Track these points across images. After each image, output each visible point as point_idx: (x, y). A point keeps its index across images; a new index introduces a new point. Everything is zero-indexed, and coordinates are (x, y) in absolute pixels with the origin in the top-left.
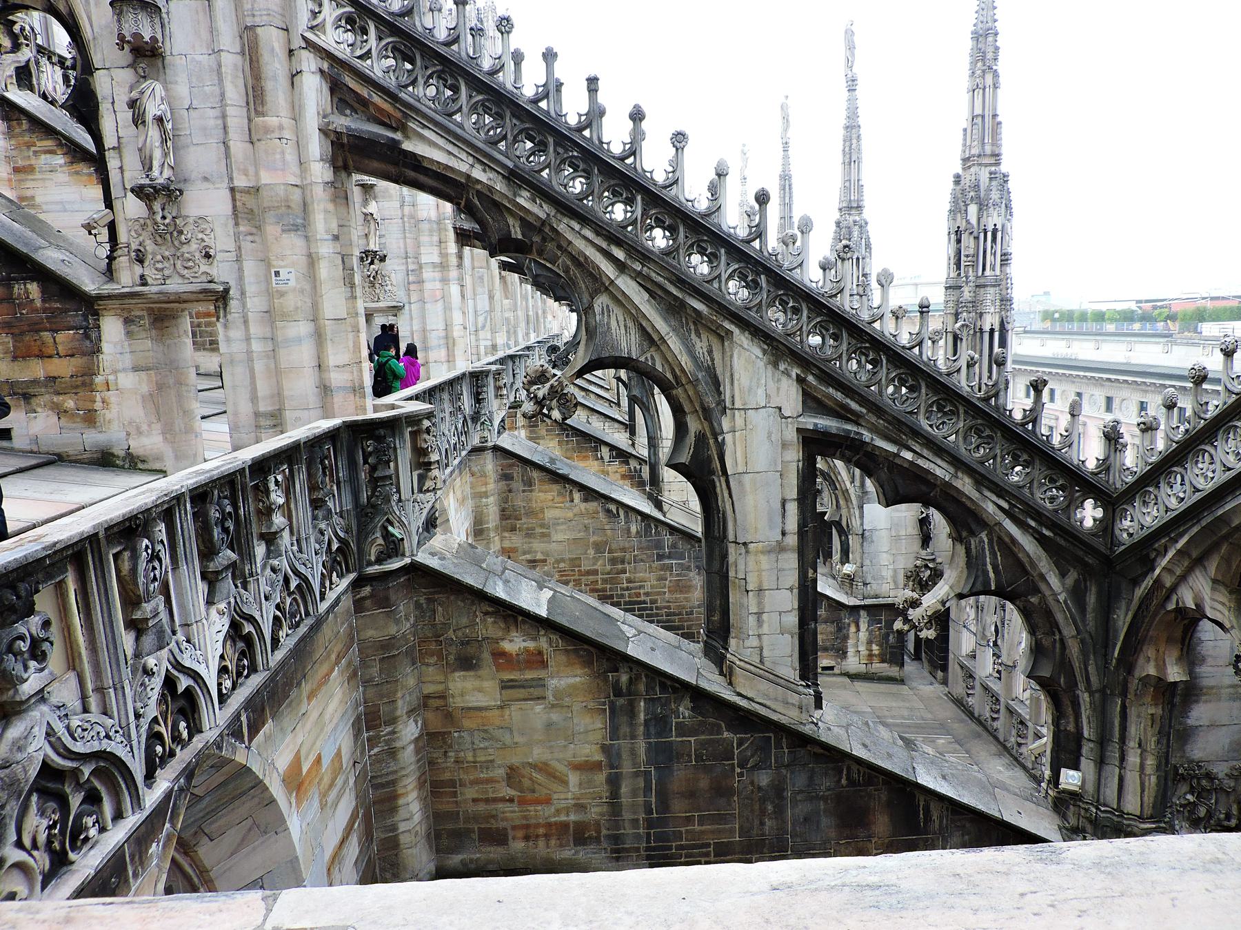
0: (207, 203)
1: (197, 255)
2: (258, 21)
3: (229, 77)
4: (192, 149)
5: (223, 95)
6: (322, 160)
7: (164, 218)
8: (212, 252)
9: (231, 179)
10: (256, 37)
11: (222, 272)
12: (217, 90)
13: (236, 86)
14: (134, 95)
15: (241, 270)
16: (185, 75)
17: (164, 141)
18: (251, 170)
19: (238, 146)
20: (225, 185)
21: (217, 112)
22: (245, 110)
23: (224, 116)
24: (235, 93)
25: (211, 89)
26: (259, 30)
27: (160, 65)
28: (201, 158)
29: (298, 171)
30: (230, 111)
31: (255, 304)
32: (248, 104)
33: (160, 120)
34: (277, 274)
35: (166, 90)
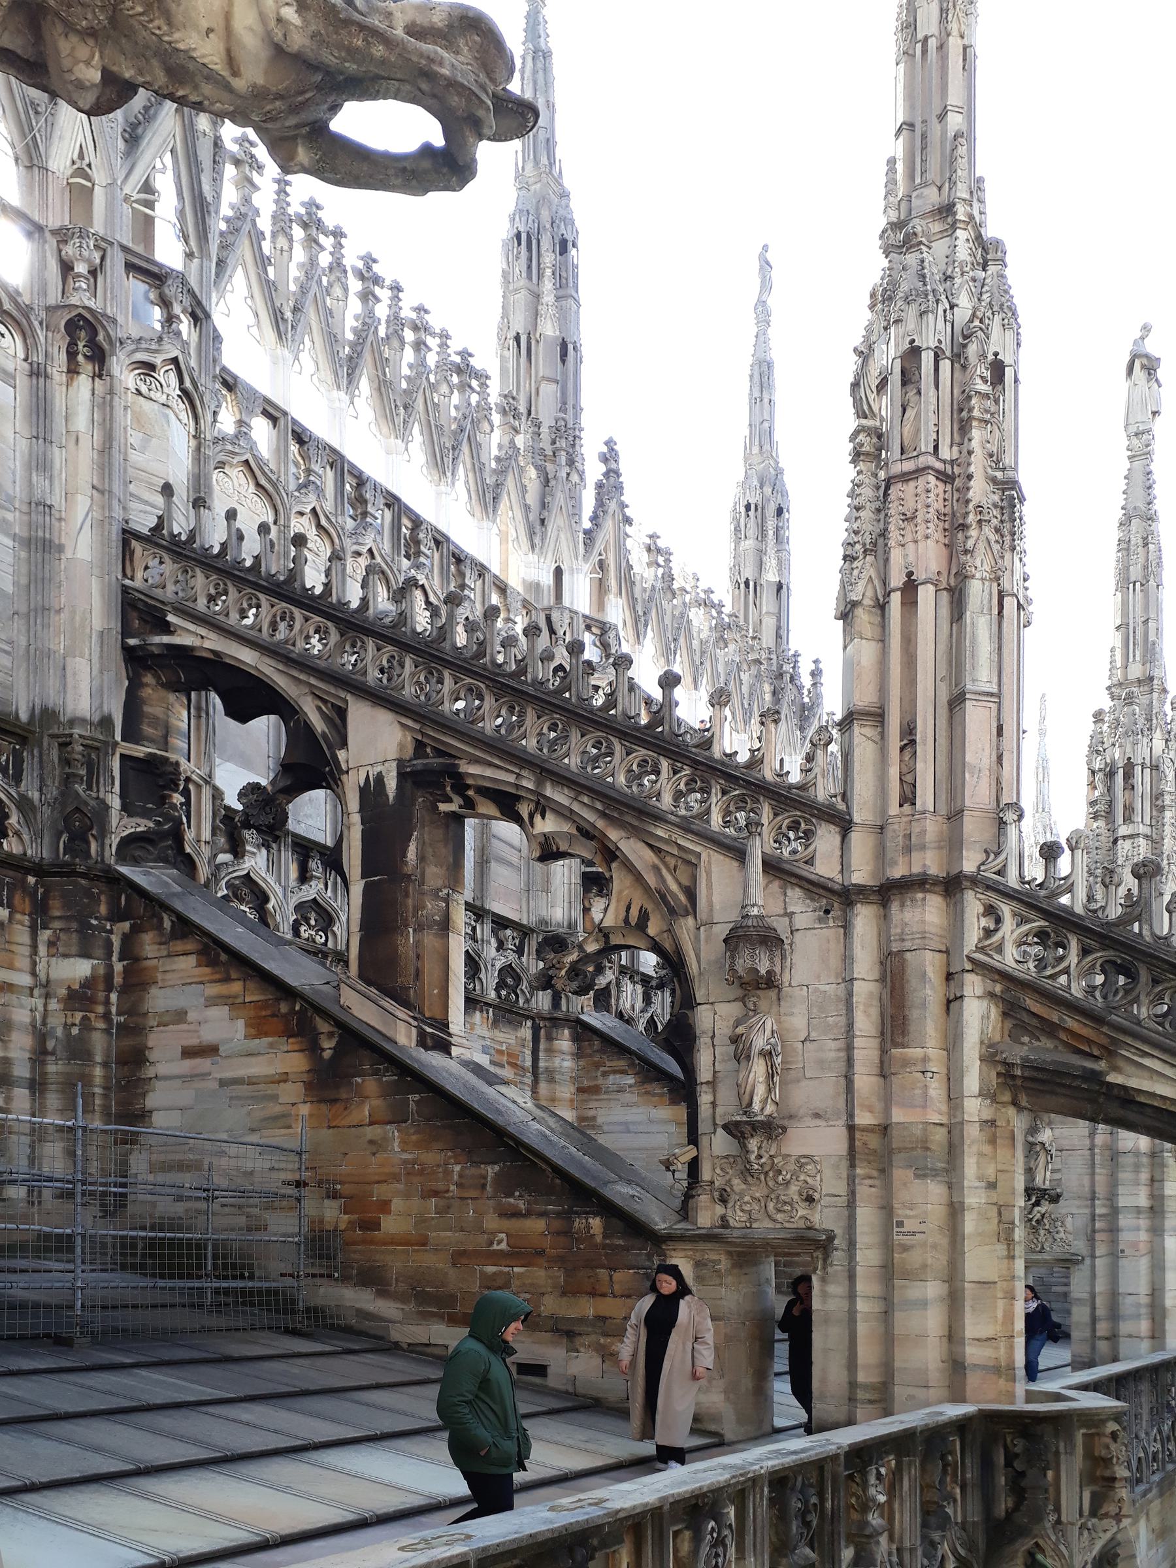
0: (817, 1142)
1: (796, 1198)
2: (908, 945)
3: (861, 1007)
4: (804, 1083)
5: (850, 1026)
6: (980, 1095)
7: (760, 1157)
8: (816, 1196)
9: (851, 1115)
10: (903, 962)
11: (825, 1218)
12: (843, 1021)
13: (869, 1016)
14: (740, 1030)
15: (852, 1218)
16: (804, 1007)
17: (770, 1077)
18: (879, 1106)
19: (865, 1081)
20: (842, 1122)
21: (841, 1044)
22: (878, 1040)
23: (849, 1048)
24: (866, 1023)
25: (836, 1019)
26: (908, 955)
27: (774, 997)
28: (815, 1090)
29: (944, 1108)
30: (858, 1042)
31: (868, 1257)
32: (882, 1034)
33: (767, 1055)
34: (900, 1224)
35: (779, 1022)
